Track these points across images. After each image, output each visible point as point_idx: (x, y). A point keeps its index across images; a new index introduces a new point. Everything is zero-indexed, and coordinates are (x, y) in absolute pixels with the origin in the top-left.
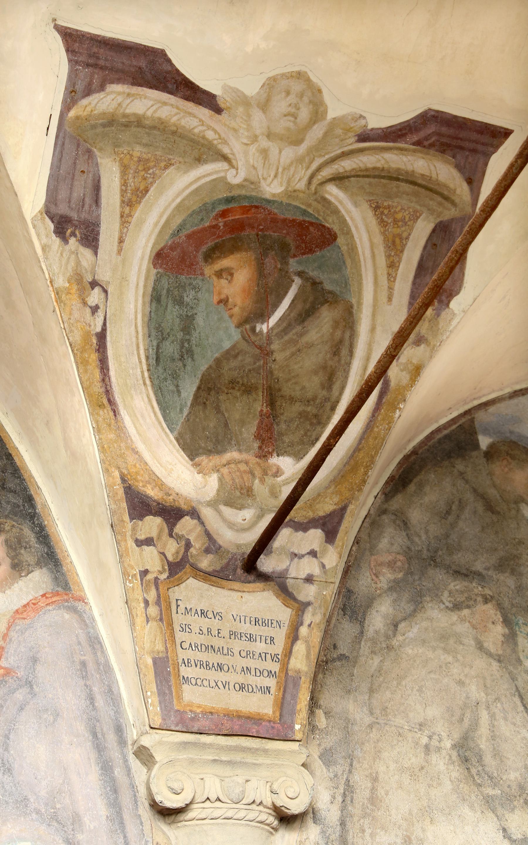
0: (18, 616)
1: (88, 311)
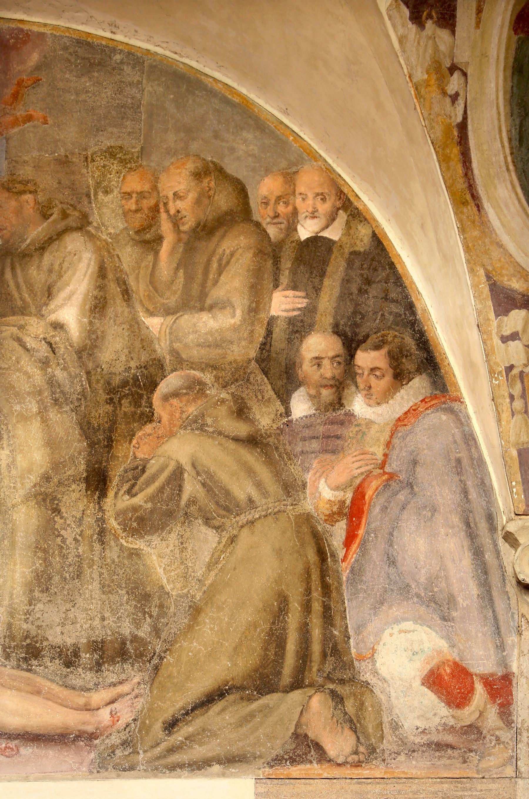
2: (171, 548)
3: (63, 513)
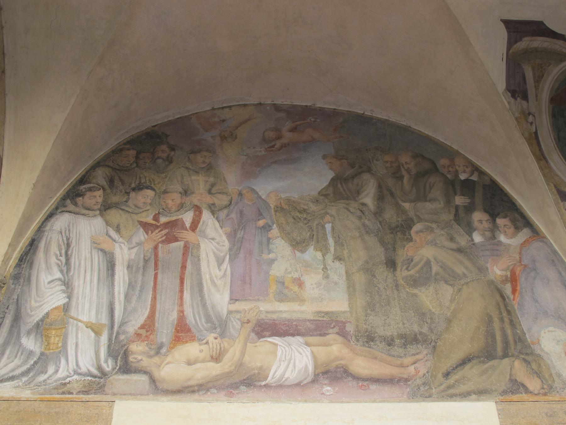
0: (523, 246)
1: (529, 124)
2: (431, 293)
3: (377, 277)
